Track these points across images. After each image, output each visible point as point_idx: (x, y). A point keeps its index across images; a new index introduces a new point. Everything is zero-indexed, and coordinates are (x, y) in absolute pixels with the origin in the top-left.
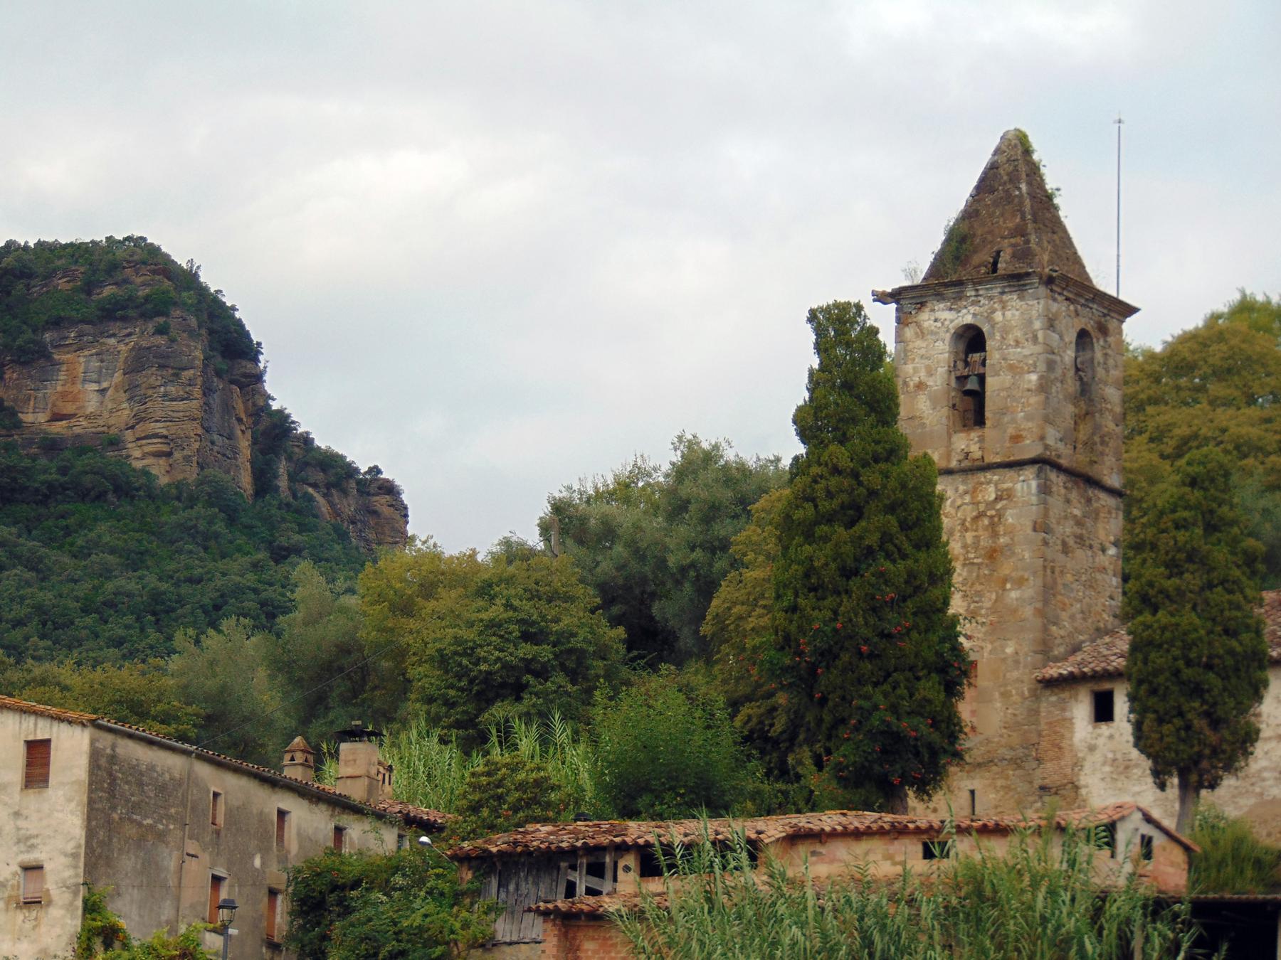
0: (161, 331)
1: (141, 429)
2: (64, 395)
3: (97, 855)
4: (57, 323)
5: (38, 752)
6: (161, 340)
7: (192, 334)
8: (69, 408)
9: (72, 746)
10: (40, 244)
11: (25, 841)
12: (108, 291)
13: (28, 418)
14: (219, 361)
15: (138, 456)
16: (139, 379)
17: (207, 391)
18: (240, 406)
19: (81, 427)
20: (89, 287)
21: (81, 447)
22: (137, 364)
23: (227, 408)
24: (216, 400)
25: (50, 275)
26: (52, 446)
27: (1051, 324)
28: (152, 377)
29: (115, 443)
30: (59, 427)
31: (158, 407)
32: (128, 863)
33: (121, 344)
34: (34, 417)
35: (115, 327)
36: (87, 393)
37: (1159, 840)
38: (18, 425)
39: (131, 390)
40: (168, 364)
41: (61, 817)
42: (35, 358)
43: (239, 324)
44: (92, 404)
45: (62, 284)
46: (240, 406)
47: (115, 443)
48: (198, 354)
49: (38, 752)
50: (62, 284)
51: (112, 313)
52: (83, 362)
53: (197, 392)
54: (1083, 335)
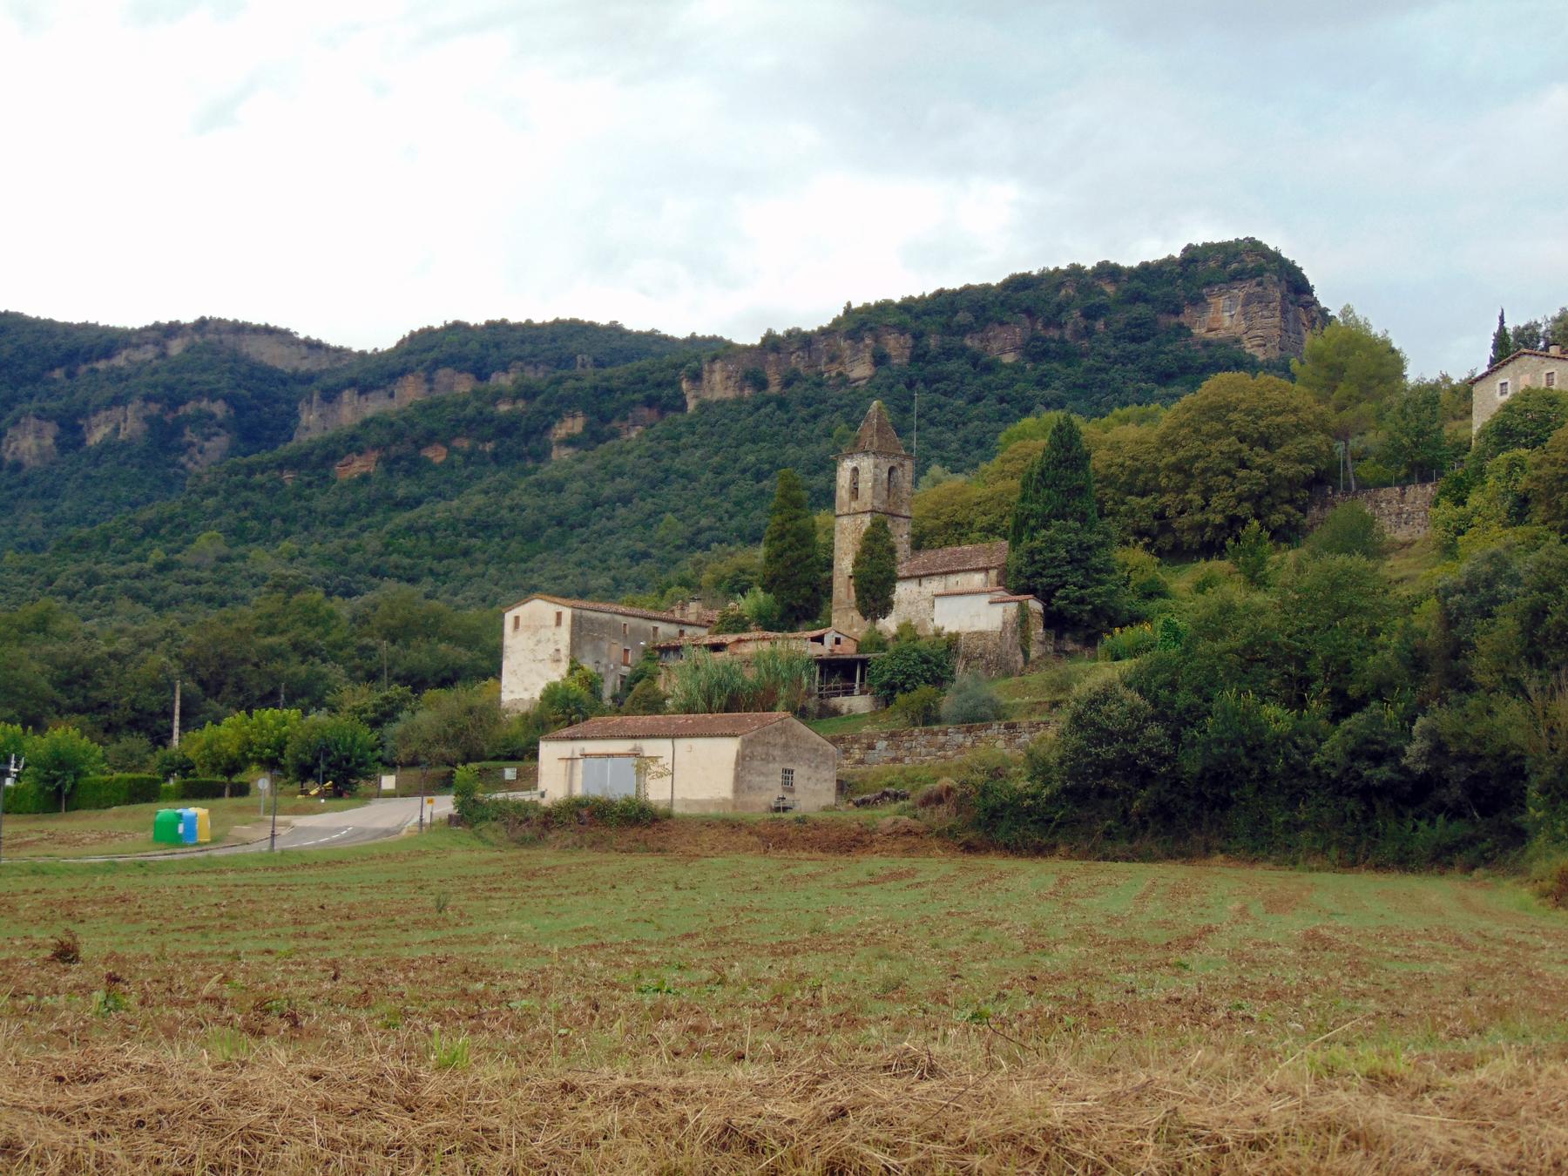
0: (1259, 284)
1: (1251, 334)
2: (1213, 319)
3: (574, 646)
4: (1208, 284)
5: (559, 615)
6: (1259, 289)
7: (1275, 285)
8: (1215, 325)
9: (567, 613)
10: (1204, 244)
11: (556, 642)
12: (1234, 266)
13: (1195, 331)
14: (1292, 296)
15: (1249, 347)
16: (1249, 309)
17: (1284, 312)
18: (1304, 318)
19: (1222, 334)
20: (1225, 265)
21: (1222, 344)
22: (1247, 302)
23: (1297, 319)
24: (1290, 316)
25: (1206, 261)
26: (1207, 344)
27: (876, 467)
28: (1255, 307)
29: (1238, 341)
30: (1211, 335)
31: (1258, 322)
32: (588, 648)
33: (1239, 292)
34: (1199, 331)
35: (1236, 284)
36: (1221, 316)
37: (843, 638)
38: (1191, 335)
39: (1245, 314)
40: (1262, 300)
41: (564, 635)
42: (1198, 301)
43: (1304, 277)
44: (1227, 323)
45: (1212, 264)
46: (1304, 318)
47: (1238, 341)
48: (1278, 294)
49: (559, 615)
50: (1212, 264)
51: (1237, 277)
52: (1222, 302)
53: (1278, 313)
54: (891, 470)
